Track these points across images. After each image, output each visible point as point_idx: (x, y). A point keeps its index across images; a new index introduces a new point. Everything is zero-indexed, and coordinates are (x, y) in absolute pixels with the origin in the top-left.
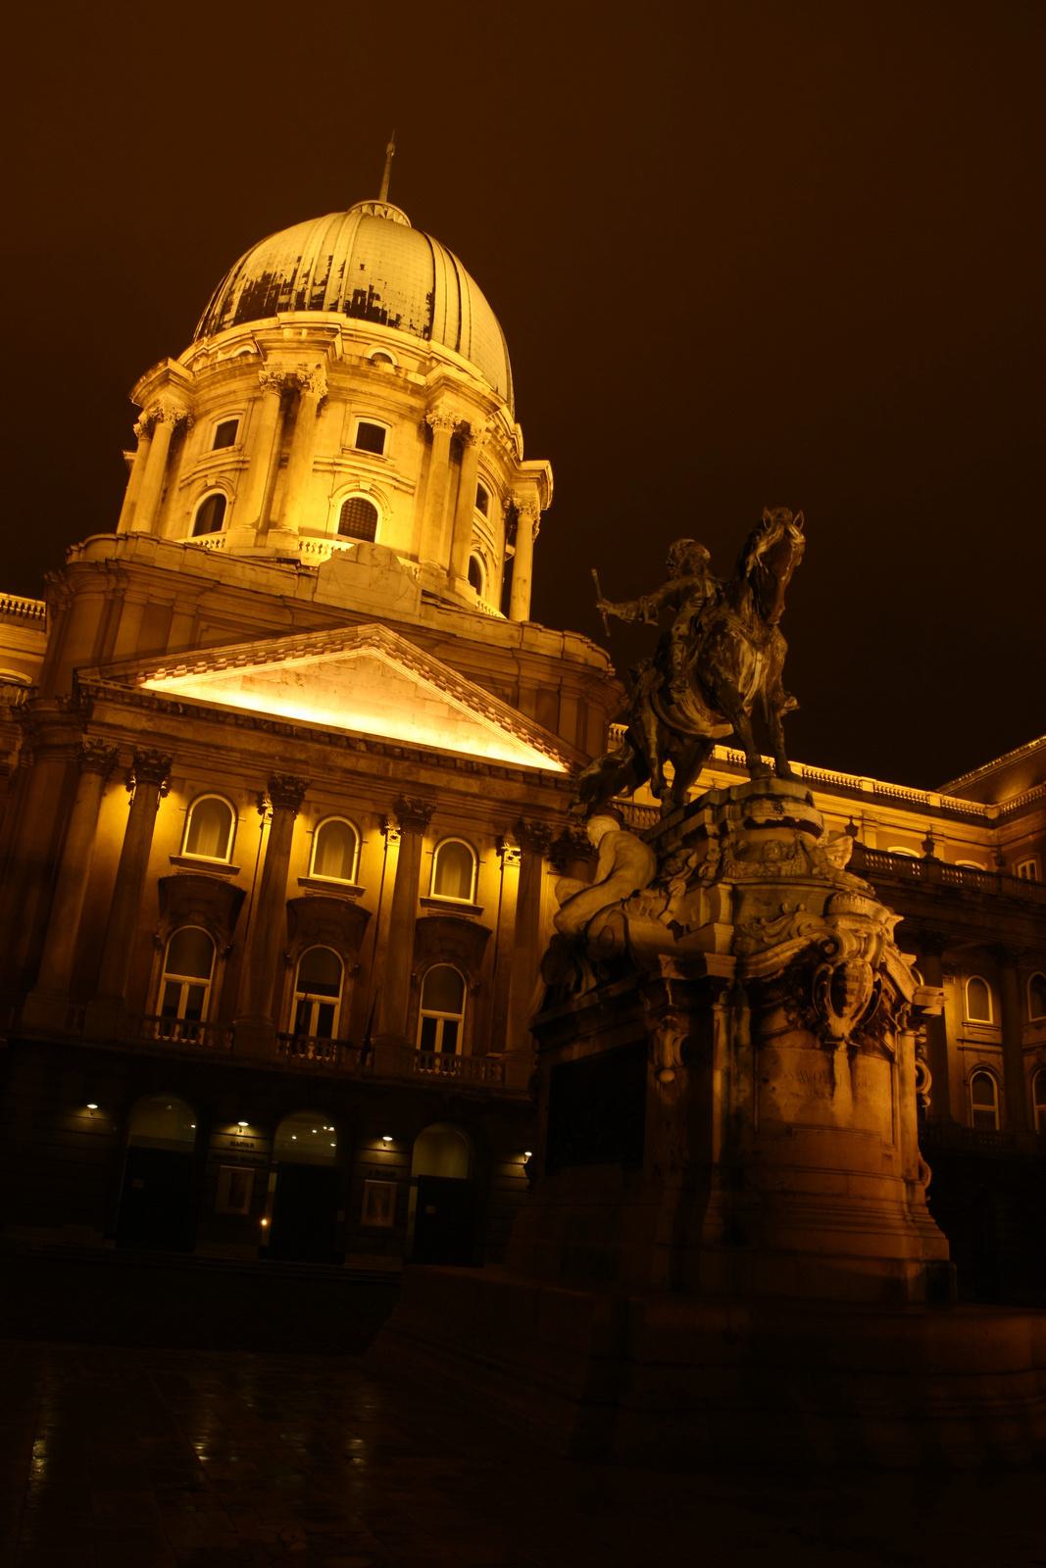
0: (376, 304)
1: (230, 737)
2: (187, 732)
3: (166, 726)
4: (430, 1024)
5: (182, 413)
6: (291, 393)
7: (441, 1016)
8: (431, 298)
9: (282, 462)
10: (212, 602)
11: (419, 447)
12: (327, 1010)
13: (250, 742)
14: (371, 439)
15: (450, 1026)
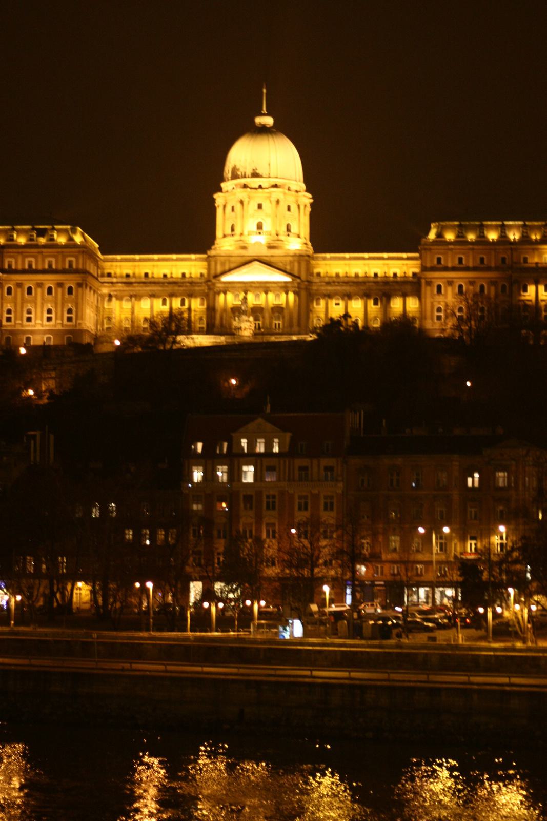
0: (257, 172)
1: (236, 285)
2: (229, 285)
3: (227, 285)
4: (276, 324)
5: (224, 204)
6: (242, 202)
7: (277, 322)
8: (269, 165)
9: (243, 217)
10: (232, 259)
11: (270, 205)
12: (259, 324)
13: (239, 285)
14: (260, 206)
15: (279, 324)
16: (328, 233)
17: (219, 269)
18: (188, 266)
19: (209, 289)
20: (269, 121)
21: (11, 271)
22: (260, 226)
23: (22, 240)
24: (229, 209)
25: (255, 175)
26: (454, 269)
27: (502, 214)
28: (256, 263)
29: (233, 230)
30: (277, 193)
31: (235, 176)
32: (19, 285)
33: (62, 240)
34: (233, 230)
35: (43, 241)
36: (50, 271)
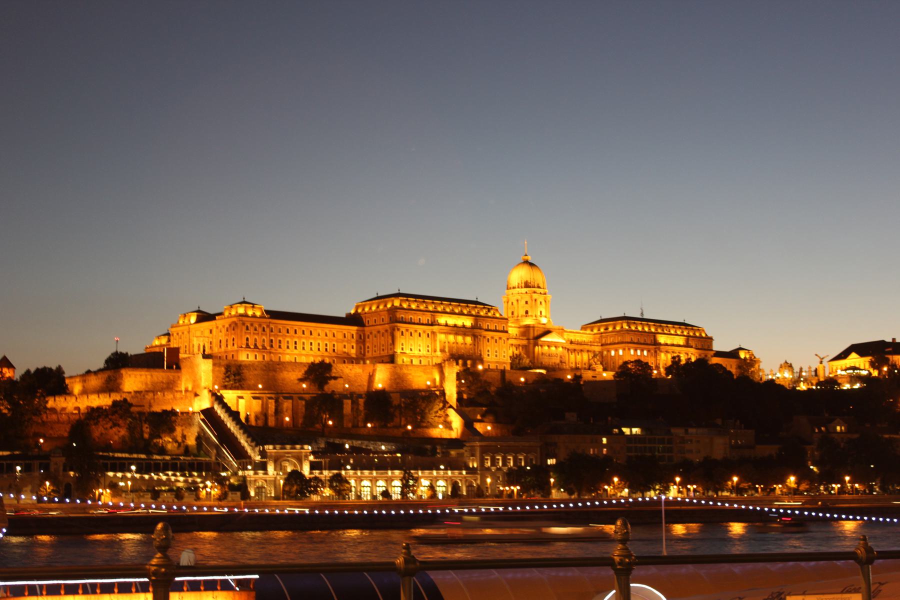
17: (536, 334)
19: (529, 343)
23: (482, 313)
25: (539, 287)
28: (553, 334)
29: (527, 312)
31: (527, 285)
32: (484, 337)
34: (527, 312)
36: (496, 331)
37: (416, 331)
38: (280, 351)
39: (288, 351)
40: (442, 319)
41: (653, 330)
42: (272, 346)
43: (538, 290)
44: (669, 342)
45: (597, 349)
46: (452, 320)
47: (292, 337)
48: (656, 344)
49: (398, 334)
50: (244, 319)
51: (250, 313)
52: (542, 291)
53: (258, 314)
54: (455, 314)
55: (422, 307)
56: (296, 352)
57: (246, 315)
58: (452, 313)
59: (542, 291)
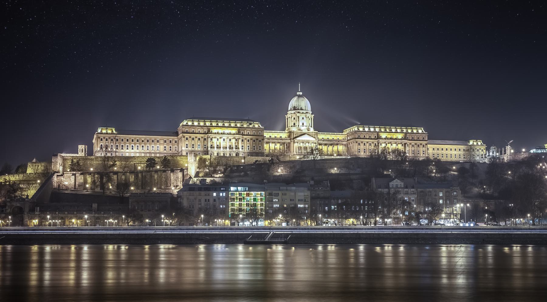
14: (303, 118)
16: (319, 127)
18: (284, 135)
20: (301, 93)
21: (243, 135)
22: (303, 124)
23: (245, 126)
24: (293, 118)
25: (301, 109)
26: (363, 139)
27: (374, 124)
29: (294, 124)
30: (308, 115)
31: (295, 108)
33: (256, 126)
34: (294, 124)
35: (251, 126)
37: (196, 137)
38: (122, 151)
39: (127, 151)
40: (214, 130)
41: (377, 130)
42: (117, 149)
43: (301, 111)
44: (389, 136)
45: (344, 143)
46: (220, 131)
47: (130, 144)
48: (379, 138)
49: (183, 139)
50: (99, 135)
51: (104, 131)
52: (304, 112)
53: (109, 132)
54: (232, 127)
55: (202, 124)
56: (132, 151)
57: (101, 133)
58: (224, 126)
59: (304, 112)
